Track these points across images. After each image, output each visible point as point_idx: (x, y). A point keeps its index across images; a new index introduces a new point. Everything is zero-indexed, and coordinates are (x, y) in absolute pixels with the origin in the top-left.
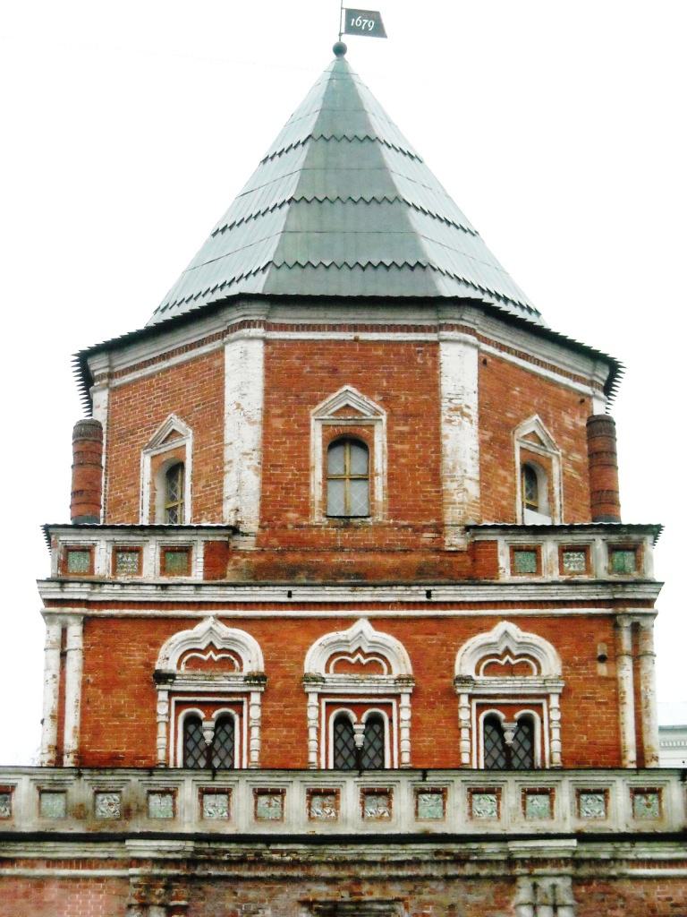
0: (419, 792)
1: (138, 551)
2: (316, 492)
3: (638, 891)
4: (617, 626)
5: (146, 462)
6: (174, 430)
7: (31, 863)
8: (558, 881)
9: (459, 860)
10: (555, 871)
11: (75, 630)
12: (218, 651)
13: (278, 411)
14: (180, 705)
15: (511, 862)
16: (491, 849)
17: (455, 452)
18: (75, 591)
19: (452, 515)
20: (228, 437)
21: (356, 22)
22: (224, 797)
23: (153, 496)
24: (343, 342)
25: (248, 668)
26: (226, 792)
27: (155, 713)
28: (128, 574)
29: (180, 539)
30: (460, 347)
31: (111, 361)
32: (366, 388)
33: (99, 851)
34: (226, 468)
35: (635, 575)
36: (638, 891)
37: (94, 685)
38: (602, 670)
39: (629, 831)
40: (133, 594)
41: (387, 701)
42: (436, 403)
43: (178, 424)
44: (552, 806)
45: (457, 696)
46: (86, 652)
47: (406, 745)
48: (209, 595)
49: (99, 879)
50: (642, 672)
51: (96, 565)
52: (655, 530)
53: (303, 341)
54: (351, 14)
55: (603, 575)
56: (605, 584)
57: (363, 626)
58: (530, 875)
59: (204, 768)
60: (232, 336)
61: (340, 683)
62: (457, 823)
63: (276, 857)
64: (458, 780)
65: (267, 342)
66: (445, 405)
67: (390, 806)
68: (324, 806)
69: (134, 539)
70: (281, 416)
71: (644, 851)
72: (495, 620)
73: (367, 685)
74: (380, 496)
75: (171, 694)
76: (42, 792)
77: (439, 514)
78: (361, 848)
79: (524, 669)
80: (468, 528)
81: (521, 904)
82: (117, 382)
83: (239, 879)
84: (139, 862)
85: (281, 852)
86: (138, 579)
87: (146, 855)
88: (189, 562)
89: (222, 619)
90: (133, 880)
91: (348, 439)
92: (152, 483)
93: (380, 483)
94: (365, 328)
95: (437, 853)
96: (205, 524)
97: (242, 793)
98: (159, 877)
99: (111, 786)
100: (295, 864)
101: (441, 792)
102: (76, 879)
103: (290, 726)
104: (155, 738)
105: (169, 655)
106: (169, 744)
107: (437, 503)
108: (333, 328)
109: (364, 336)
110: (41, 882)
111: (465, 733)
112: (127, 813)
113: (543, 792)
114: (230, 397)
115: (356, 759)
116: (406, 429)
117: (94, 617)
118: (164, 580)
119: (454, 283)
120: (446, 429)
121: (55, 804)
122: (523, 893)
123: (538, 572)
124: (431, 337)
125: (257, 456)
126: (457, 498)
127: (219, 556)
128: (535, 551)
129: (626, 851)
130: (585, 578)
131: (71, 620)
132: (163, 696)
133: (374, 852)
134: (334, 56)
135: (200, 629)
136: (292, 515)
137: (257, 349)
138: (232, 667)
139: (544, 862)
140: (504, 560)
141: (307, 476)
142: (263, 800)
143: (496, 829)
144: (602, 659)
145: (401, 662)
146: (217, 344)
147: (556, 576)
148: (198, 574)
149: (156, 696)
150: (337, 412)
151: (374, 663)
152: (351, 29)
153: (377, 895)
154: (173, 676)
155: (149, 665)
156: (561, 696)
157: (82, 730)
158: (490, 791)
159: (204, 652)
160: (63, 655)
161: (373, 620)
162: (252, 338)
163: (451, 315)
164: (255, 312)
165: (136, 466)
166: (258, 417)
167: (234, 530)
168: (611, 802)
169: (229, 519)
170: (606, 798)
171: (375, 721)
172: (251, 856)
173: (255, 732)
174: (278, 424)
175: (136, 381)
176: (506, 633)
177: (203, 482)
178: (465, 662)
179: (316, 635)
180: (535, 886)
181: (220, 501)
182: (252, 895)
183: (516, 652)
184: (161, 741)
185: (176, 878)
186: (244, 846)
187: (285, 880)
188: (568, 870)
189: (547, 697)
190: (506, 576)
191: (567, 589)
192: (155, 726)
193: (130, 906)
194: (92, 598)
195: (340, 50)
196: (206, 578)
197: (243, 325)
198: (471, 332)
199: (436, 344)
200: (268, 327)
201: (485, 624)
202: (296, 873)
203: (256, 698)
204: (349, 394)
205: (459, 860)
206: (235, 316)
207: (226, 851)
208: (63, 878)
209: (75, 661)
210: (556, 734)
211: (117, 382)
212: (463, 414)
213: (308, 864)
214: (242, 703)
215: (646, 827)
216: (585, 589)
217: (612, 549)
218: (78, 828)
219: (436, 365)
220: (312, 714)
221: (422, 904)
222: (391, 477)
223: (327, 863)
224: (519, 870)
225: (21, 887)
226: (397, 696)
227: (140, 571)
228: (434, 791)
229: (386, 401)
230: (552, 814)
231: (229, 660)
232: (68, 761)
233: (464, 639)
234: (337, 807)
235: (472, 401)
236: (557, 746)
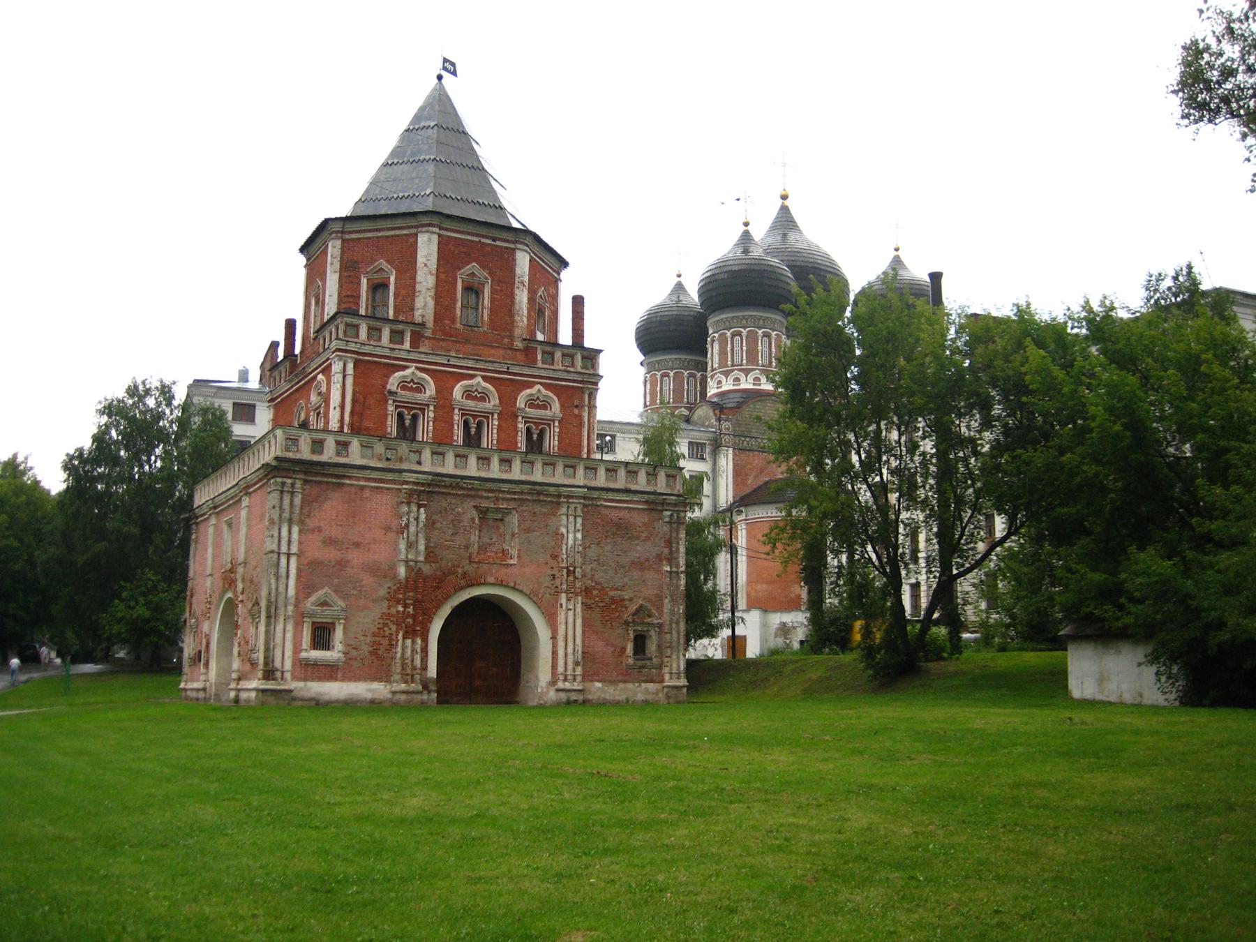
0: (523, 462)
1: (380, 330)
2: (458, 312)
3: (606, 512)
4: (583, 392)
5: (364, 281)
6: (382, 269)
7: (358, 479)
8: (578, 505)
9: (539, 493)
10: (577, 501)
11: (350, 366)
12: (415, 383)
13: (443, 270)
14: (397, 407)
15: (559, 496)
16: (552, 489)
17: (520, 303)
18: (352, 347)
19: (517, 332)
20: (419, 279)
21: (447, 65)
22: (442, 456)
23: (367, 299)
24: (473, 241)
25: (428, 393)
26: (443, 454)
27: (386, 409)
28: (375, 341)
29: (401, 327)
30: (524, 253)
31: (344, 225)
32: (483, 267)
33: (389, 476)
34: (417, 294)
35: (591, 372)
36: (606, 512)
37: (359, 393)
38: (576, 411)
39: (605, 486)
40: (378, 351)
41: (487, 415)
42: (513, 277)
43: (384, 264)
44: (575, 473)
45: (517, 417)
46: (355, 377)
47: (495, 436)
48: (413, 356)
49: (388, 489)
50: (592, 415)
51: (360, 334)
52: (600, 351)
53: (455, 237)
54: (445, 60)
55: (579, 369)
56: (581, 373)
57: (479, 379)
58: (568, 502)
59: (395, 438)
60: (424, 229)
61: (470, 404)
62: (538, 476)
63: (465, 485)
64: (539, 458)
65: (440, 236)
66: (517, 279)
67: (511, 467)
68: (483, 464)
69: (378, 324)
70: (444, 273)
71: (611, 496)
72: (534, 384)
73: (482, 406)
74: (486, 318)
75: (394, 401)
76: (362, 446)
77: (511, 331)
78: (501, 485)
79: (544, 407)
80: (525, 340)
81: (563, 514)
82: (347, 237)
83: (450, 494)
84: (407, 483)
85: (467, 484)
86: (379, 344)
87: (411, 480)
88: (403, 338)
89: (417, 368)
90: (404, 491)
91: (472, 289)
92: (367, 292)
93: (486, 313)
94: (483, 236)
95: (531, 489)
96: (401, 318)
97: (427, 454)
98: (416, 490)
99: (392, 446)
100: (472, 489)
101: (532, 463)
102: (377, 488)
103: (446, 422)
104: (386, 422)
105: (393, 382)
106: (392, 427)
107: (511, 325)
108: (469, 234)
109: (483, 240)
110: (362, 488)
111: (520, 434)
112: (401, 460)
113: (572, 467)
114: (421, 259)
115: (472, 440)
116: (498, 288)
117: (360, 360)
118: (392, 346)
119: (517, 223)
120: (517, 291)
121: (369, 452)
122: (564, 510)
123: (553, 364)
124: (512, 246)
125: (433, 290)
126: (520, 324)
127: (417, 339)
128: (552, 354)
129: (605, 495)
130: (572, 370)
131: (349, 360)
132: (390, 402)
133: (505, 487)
134: (437, 81)
135: (408, 372)
136: (447, 322)
137: (435, 238)
138: (421, 392)
139: (572, 497)
140: (539, 358)
141: (455, 304)
142: (458, 459)
143: (552, 480)
144: (577, 407)
145: (495, 400)
146: (413, 231)
147: (560, 367)
148: (407, 345)
149: (387, 401)
150: (467, 275)
151: (483, 397)
152: (445, 69)
153: (505, 506)
154: (396, 393)
155: (384, 386)
156: (559, 422)
157: (352, 413)
158: (551, 464)
159: (409, 383)
160: (344, 377)
161: (484, 378)
162: (435, 233)
163: (521, 237)
164: (436, 220)
165: (359, 284)
166: (435, 272)
167: (423, 325)
168: (598, 474)
169: (418, 319)
170: (596, 471)
171: (479, 425)
172: (454, 484)
173: (431, 423)
174: (443, 276)
175: (359, 239)
176: (539, 390)
177: (401, 298)
178: (521, 402)
179: (458, 382)
180: (568, 507)
181: (412, 309)
182: (454, 501)
183: (541, 399)
184: (389, 423)
185: (421, 491)
186: (453, 480)
187: (468, 496)
188: (582, 501)
189: (553, 421)
190: (540, 364)
191: (565, 374)
192: (387, 415)
193: (402, 503)
194: (360, 351)
195: (440, 77)
196: (411, 347)
197: (429, 225)
198: (527, 245)
199: (514, 250)
200: (441, 228)
201: (531, 385)
202: (473, 493)
203: (432, 408)
204: (474, 267)
205: (539, 493)
206: (425, 220)
207: (444, 481)
208: (372, 487)
209: (350, 381)
210: (556, 438)
211: (347, 237)
212: (524, 285)
213: (478, 490)
214: (424, 409)
215: (611, 485)
216: (573, 375)
217: (583, 358)
218: (379, 465)
219: (514, 260)
220: (456, 418)
221: (524, 511)
222: (492, 310)
223: (485, 490)
224: (562, 499)
225: (353, 490)
226: (492, 414)
227: (380, 339)
228: (529, 462)
229: (491, 274)
230: (554, 475)
231: (420, 388)
232: (346, 430)
233: (521, 391)
234: (489, 465)
235: (526, 279)
236: (556, 442)
